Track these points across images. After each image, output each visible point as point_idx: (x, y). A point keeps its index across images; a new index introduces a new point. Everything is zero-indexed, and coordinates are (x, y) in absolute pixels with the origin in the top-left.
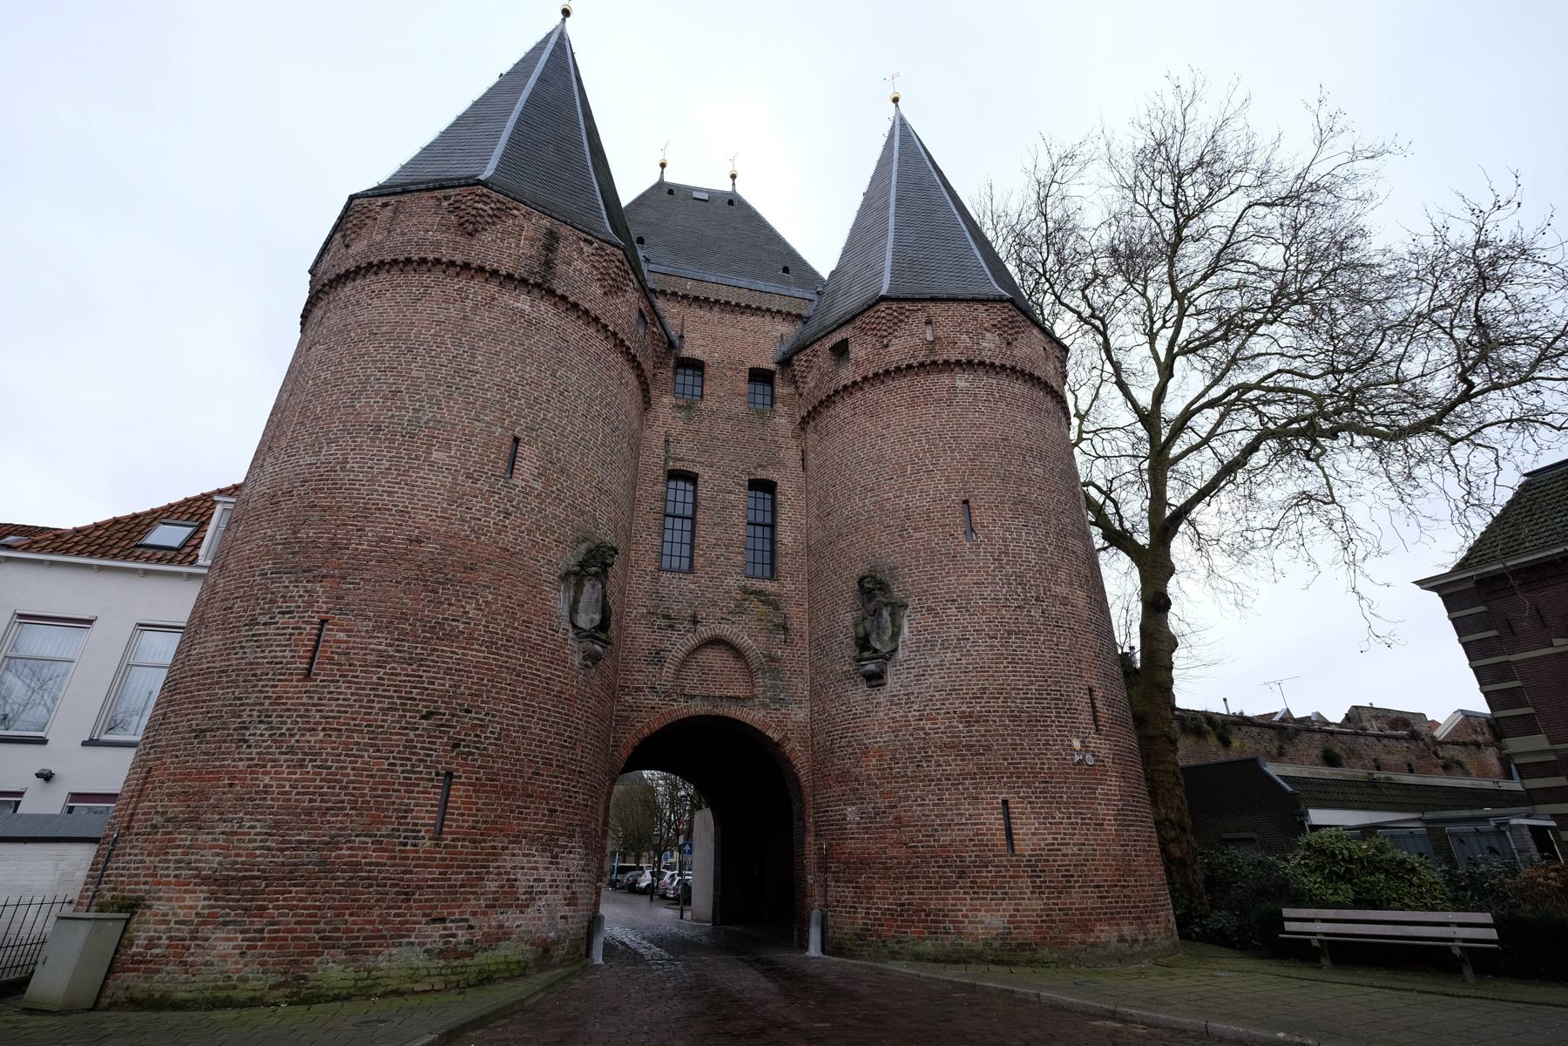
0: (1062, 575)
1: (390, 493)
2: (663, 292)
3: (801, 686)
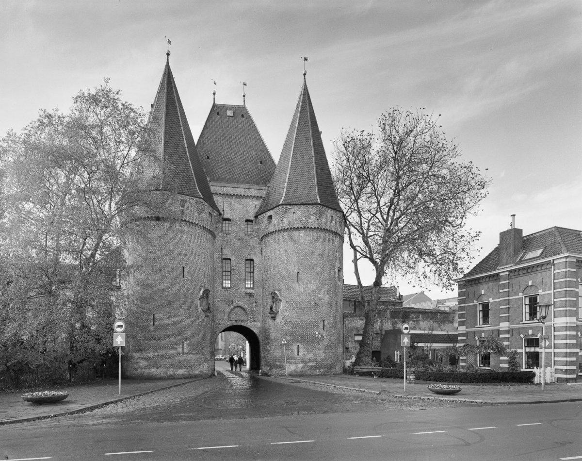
0: (322, 292)
1: (160, 285)
2: (217, 193)
3: (260, 318)
